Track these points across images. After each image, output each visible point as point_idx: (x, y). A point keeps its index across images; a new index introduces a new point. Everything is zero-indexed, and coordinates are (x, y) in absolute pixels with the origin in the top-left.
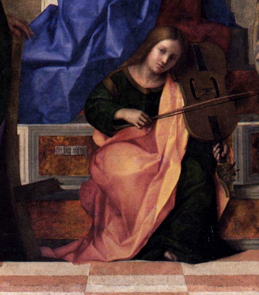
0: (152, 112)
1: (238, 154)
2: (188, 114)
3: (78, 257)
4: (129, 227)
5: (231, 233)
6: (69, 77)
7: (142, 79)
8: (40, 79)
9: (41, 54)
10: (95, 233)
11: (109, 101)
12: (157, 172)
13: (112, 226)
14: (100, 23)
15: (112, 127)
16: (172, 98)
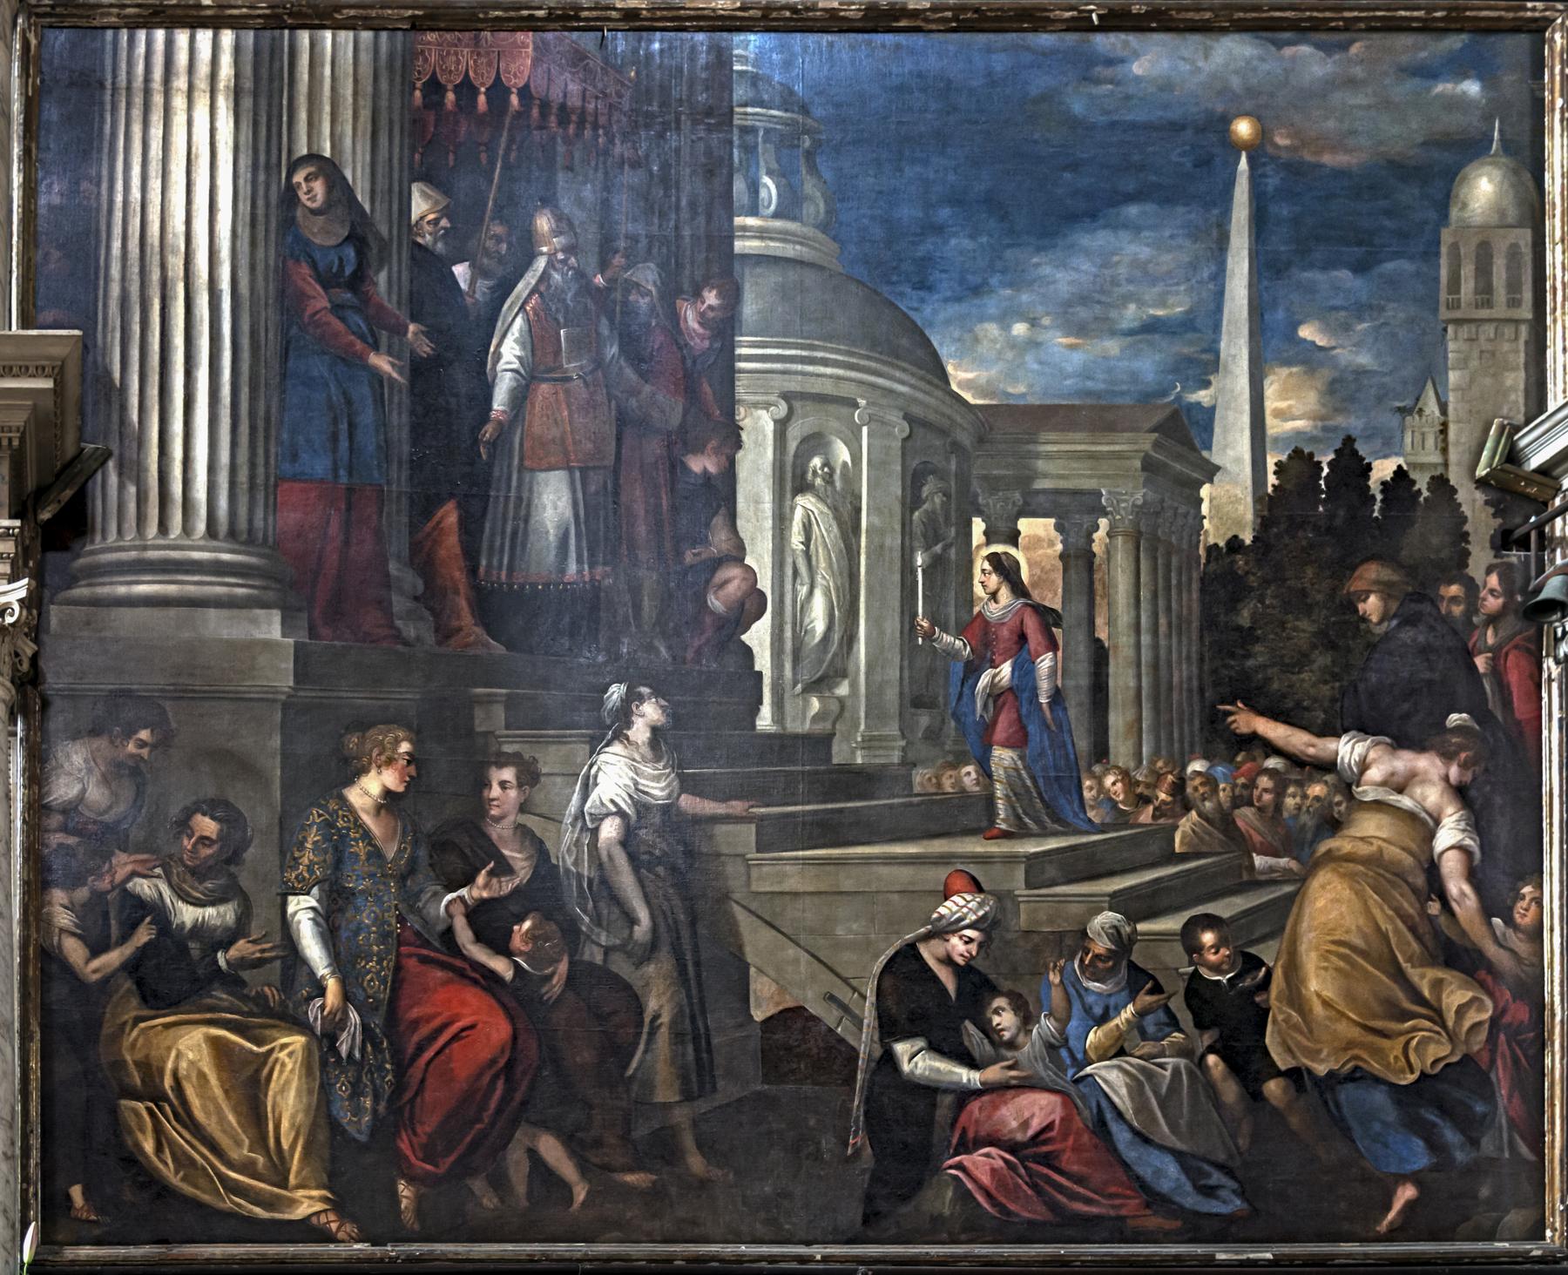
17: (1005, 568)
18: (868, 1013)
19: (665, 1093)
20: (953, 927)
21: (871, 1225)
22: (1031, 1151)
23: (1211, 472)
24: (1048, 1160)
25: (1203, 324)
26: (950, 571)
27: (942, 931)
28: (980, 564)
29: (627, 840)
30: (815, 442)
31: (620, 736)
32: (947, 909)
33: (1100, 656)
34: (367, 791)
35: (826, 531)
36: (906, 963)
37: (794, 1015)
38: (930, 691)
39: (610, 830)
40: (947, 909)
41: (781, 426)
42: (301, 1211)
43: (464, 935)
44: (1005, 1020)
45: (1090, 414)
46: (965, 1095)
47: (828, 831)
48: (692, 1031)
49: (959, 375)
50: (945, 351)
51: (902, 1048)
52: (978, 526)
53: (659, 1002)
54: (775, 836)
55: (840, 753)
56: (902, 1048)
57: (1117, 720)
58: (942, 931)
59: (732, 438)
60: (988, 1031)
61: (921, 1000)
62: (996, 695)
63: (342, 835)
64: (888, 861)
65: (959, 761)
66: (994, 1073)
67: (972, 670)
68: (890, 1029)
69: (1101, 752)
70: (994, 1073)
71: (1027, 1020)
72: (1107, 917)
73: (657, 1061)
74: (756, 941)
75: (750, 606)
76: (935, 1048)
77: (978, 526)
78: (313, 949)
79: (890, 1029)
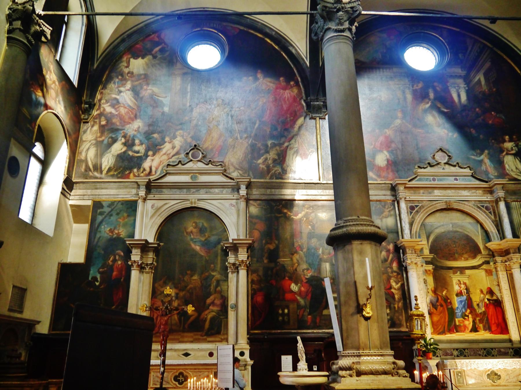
1: (477, 321)
2: (472, 317)
3: (464, 332)
4: (468, 329)
5: (478, 330)
6: (460, 314)
7: (467, 314)
8: (457, 314)
10: (465, 330)
11: (464, 316)
12: (470, 324)
13: (466, 329)
15: (465, 319)
16: (470, 316)
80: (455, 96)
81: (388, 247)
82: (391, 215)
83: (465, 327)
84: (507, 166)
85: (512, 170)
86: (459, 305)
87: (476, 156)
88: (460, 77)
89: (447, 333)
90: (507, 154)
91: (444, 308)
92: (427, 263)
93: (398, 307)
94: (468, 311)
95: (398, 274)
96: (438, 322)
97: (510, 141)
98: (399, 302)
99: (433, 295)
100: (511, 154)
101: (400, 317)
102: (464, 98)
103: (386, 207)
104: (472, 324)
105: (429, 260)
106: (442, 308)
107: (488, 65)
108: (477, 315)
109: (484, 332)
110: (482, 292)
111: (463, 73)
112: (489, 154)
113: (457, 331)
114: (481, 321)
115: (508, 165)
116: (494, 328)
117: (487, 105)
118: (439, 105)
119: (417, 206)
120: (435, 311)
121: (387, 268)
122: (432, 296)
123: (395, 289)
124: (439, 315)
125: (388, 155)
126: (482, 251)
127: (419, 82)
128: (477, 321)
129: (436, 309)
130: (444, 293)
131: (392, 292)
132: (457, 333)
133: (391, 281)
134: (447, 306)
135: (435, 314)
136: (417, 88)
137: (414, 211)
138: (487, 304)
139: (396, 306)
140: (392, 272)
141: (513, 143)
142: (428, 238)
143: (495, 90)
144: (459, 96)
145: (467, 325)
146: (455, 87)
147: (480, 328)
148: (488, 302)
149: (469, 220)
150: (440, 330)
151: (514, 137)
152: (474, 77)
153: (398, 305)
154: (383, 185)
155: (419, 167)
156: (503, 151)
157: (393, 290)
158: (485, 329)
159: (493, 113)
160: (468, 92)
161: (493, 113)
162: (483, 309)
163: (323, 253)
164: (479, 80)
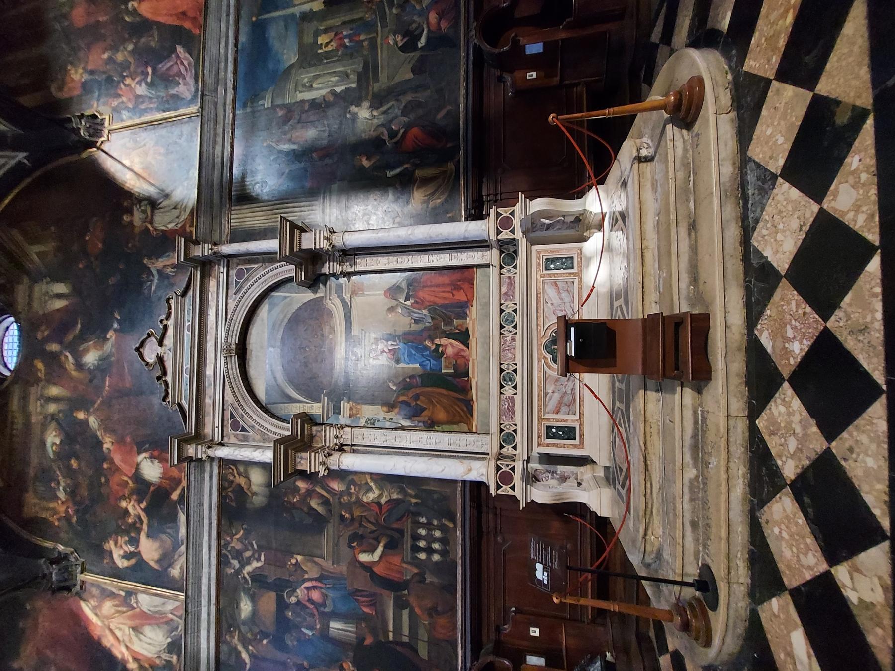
0: (440, 345)
3: (468, 361)
4: (463, 350)
5: (464, 329)
7: (433, 347)
9: (428, 367)
10: (464, 357)
11: (438, 354)
12: (451, 344)
13: (463, 354)
14: (423, 356)
15: (443, 353)
16: (437, 341)
17: (327, 44)
18: (412, 54)
19: (428, 93)
20: (395, 40)
21: (456, 46)
22: (441, 16)
23: (311, 10)
24: (443, 12)
25: (286, 18)
26: (328, 55)
27: (396, 43)
28: (326, 49)
29: (377, 109)
30: (304, 86)
31: (356, 114)
32: (391, 43)
33: (344, 23)
34: (366, 163)
35: (319, 80)
36: (403, 49)
37: (413, 70)
38: (349, 54)
39: (375, 113)
40: (391, 43)
41: (300, 92)
42: (454, 167)
43: (394, 140)
44: (414, 26)
45: (300, 34)
46: (429, 31)
47: (376, 67)
48: (415, 90)
49: (293, 61)
50: (287, 64)
51: (420, 45)
52: (320, 51)
53: (409, 97)
54: (377, 79)
55: (360, 69)
56: (420, 45)
57: (355, 17)
58: (396, 43)
59: (303, 101)
60: (416, 29)
61: (409, 46)
62: (350, 41)
63: (375, 168)
64: (382, 56)
65: (363, 46)
66: (425, 27)
67: (345, 46)
68: (415, 48)
69: (361, 19)
70: (425, 27)
71: (414, 22)
72: (394, 11)
73: (422, 96)
74: (397, 79)
75: (333, 93)
76: (419, 39)
77: (320, 51)
78: (398, 171)
79: (415, 48)
80: (59, 304)
81: (303, 491)
82: (246, 471)
83: (458, 355)
84: (170, 226)
85: (177, 217)
86: (415, 362)
87: (151, 281)
88: (31, 289)
89: (469, 397)
90: (151, 223)
91: (421, 394)
92: (337, 411)
93: (415, 497)
94: (428, 343)
95: (353, 482)
96: (447, 411)
97: (130, 212)
98: (406, 494)
99: (396, 410)
100: (152, 216)
101: (435, 496)
102: (61, 288)
103: (232, 478)
104: (451, 341)
105: (331, 405)
106: (421, 397)
107: (16, 234)
108: (436, 327)
109: (468, 319)
110: (391, 309)
111: (26, 280)
112: (150, 258)
113: (467, 374)
114: (448, 321)
115: (170, 223)
116: (461, 296)
117: (75, 247)
118: (70, 337)
119: (232, 416)
120: (425, 413)
121: (340, 502)
122: (398, 413)
123: (381, 496)
124: (434, 406)
125: (144, 455)
126: (318, 295)
127: (35, 367)
128: (447, 328)
129: (423, 409)
130: (394, 388)
131: (386, 502)
132: (471, 375)
133: (365, 500)
134: (417, 386)
135: (432, 413)
136: (43, 372)
137: (241, 423)
138: (416, 302)
139: (414, 500)
140: (350, 494)
141: (135, 209)
142: (292, 400)
143: (53, 228)
144: (59, 296)
145: (456, 351)
146: (46, 302)
147: (461, 325)
148: (412, 301)
149: (263, 311)
150: (463, 410)
151: (125, 204)
152: (32, 262)
153: (411, 495)
154: (192, 478)
155: (164, 400)
156: (147, 229)
157: (383, 500)
158: (464, 316)
159: (87, 238)
160: (56, 279)
161: (87, 238)
162: (425, 312)
163: (311, 628)
164: (38, 254)
